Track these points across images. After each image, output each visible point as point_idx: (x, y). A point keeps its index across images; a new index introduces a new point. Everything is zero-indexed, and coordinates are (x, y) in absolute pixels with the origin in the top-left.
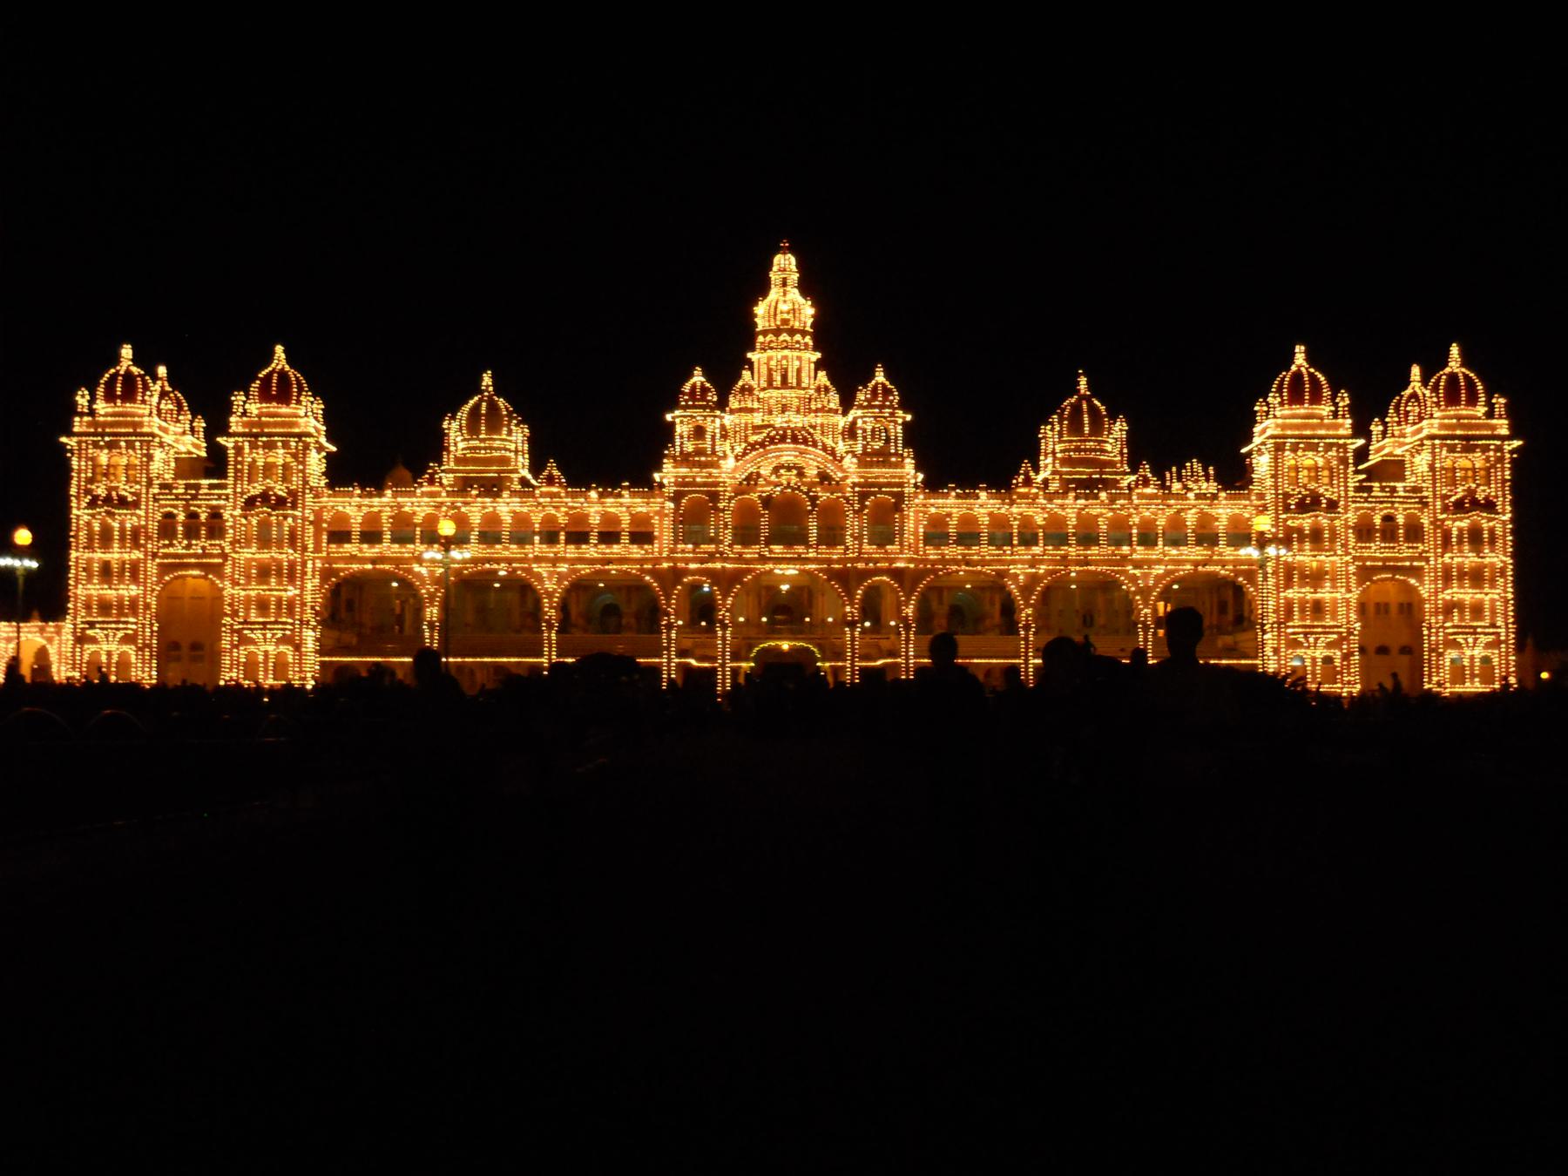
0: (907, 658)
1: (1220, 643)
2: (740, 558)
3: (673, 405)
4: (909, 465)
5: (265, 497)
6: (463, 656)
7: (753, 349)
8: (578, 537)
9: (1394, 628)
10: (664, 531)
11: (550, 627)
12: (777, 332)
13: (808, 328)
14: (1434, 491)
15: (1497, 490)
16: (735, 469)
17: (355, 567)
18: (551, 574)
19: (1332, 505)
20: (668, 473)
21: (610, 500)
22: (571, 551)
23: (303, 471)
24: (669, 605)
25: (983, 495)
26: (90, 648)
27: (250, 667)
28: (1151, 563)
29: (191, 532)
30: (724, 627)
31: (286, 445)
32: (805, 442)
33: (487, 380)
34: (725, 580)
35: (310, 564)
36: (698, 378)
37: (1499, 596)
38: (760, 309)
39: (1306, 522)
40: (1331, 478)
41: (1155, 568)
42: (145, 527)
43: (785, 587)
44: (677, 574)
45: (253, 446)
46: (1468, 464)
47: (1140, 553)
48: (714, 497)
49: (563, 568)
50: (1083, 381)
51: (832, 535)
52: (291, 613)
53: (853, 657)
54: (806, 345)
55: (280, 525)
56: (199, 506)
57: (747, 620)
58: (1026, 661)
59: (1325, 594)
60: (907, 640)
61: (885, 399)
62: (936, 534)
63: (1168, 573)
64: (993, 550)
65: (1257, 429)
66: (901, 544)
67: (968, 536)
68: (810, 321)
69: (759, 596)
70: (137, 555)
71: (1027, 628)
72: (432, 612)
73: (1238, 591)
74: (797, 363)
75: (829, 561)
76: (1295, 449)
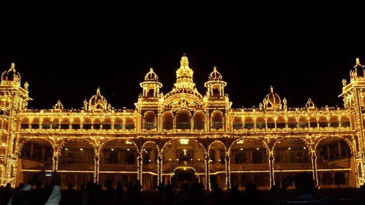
0: (228, 171)
2: (166, 135)
4: (227, 99)
7: (175, 82)
8: (107, 126)
12: (182, 77)
13: (192, 77)
16: (164, 102)
17: (31, 137)
18: (98, 140)
20: (140, 104)
21: (119, 113)
22: (104, 132)
24: (140, 152)
25: (254, 110)
28: (316, 133)
31: (7, 94)
32: (189, 92)
33: (98, 91)
36: (152, 71)
38: (178, 72)
41: (313, 136)
43: (185, 151)
47: (311, 129)
48: (156, 112)
50: (272, 89)
51: (199, 125)
54: (191, 81)
57: (173, 161)
58: (272, 171)
62: (237, 124)
63: (321, 137)
64: (258, 130)
67: (249, 125)
69: (177, 153)
71: (271, 159)
72: (56, 154)
75: (198, 135)
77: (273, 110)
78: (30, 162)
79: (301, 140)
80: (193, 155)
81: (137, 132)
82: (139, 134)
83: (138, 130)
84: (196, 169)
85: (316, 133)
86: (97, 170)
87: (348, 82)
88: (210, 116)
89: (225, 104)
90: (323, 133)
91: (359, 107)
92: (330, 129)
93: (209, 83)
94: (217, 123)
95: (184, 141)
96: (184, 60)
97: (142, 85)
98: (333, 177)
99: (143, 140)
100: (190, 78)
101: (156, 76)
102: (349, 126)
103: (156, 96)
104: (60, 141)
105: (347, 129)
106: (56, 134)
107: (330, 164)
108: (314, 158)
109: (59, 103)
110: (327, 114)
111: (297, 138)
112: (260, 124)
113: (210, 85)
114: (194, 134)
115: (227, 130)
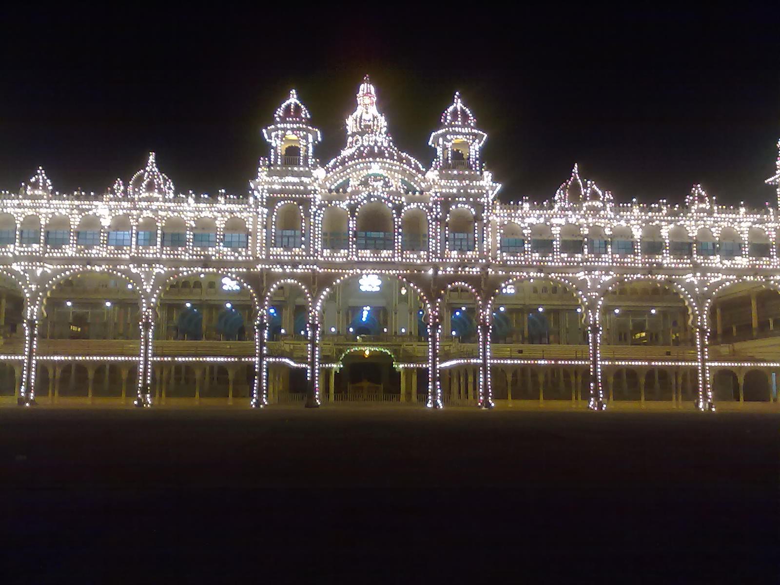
0: (485, 359)
4: (488, 175)
6: (74, 355)
12: (362, 134)
16: (326, 179)
18: (148, 275)
20: (264, 181)
24: (262, 307)
30: (314, 327)
34: (316, 282)
36: (293, 99)
48: (306, 203)
49: (159, 269)
57: (338, 333)
58: (595, 363)
67: (544, 245)
72: (32, 311)
84: (395, 352)
86: (146, 353)
93: (444, 135)
95: (370, 283)
98: (741, 380)
99: (272, 278)
101: (305, 113)
103: (306, 164)
104: (45, 277)
107: (725, 349)
108: (703, 332)
109: (41, 176)
114: (400, 263)
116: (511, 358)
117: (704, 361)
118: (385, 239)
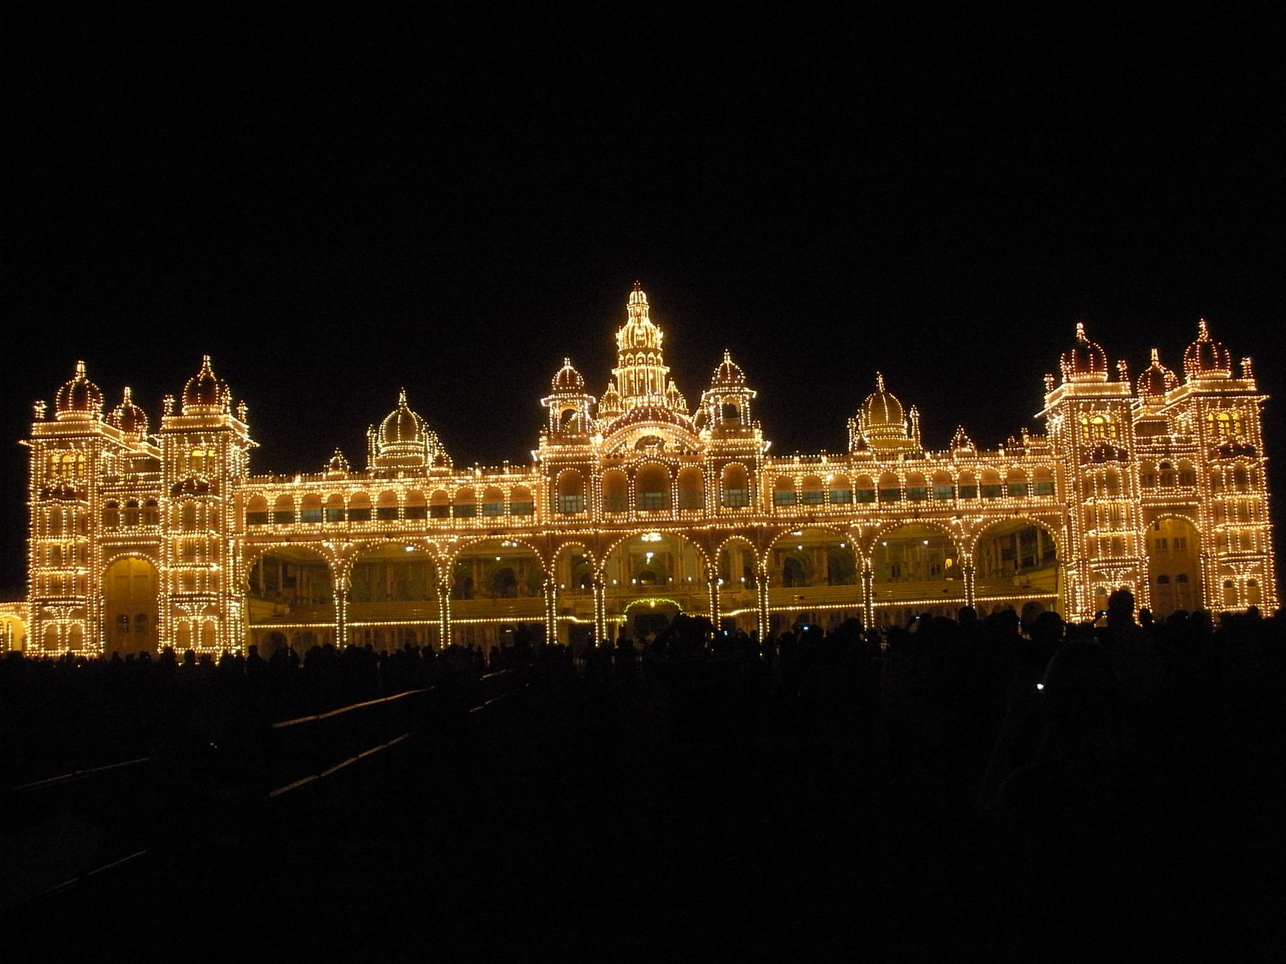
0: (763, 607)
1: (1017, 582)
2: (611, 525)
3: (547, 391)
4: (758, 434)
5: (189, 486)
8: (466, 511)
9: (1175, 563)
10: (542, 501)
11: (444, 591)
12: (635, 351)
14: (1202, 441)
15: (1251, 437)
16: (604, 444)
18: (443, 546)
19: (1123, 456)
20: (545, 451)
22: (460, 523)
23: (223, 461)
25: (824, 459)
26: (47, 623)
27: (183, 636)
28: (973, 513)
29: (131, 520)
30: (599, 587)
31: (208, 440)
32: (665, 418)
33: (402, 397)
35: (232, 543)
36: (568, 367)
37: (1261, 527)
38: (620, 335)
39: (1101, 469)
40: (1118, 432)
41: (969, 518)
42: (91, 515)
43: (650, 555)
44: (554, 542)
45: (180, 441)
46: (1227, 418)
47: (961, 503)
48: (586, 470)
50: (880, 380)
51: (692, 500)
52: (216, 587)
53: (715, 608)
55: (203, 509)
56: (136, 496)
57: (619, 583)
58: (868, 605)
59: (1123, 533)
60: (763, 591)
61: (733, 380)
63: (985, 521)
64: (836, 507)
65: (1047, 397)
66: (755, 506)
68: (660, 343)
69: (629, 562)
70: (83, 539)
71: (867, 575)
72: (340, 583)
73: (1044, 532)
74: (651, 376)
75: (690, 524)
76: (1086, 409)
77: (870, 458)
78: (264, 604)
79: (940, 529)
80: (671, 568)
81: (539, 521)
82: (547, 527)
83: (544, 516)
85: (973, 513)
86: (445, 617)
87: (1057, 384)
88: (718, 476)
89: (751, 445)
90: (991, 511)
91: (1075, 448)
92: (1006, 502)
93: (714, 395)
94: (735, 491)
96: (638, 301)
97: (547, 402)
98: (1019, 613)
100: (656, 351)
101: (579, 380)
102: (1054, 494)
103: (584, 430)
105: (1047, 501)
106: (340, 535)
108: (969, 570)
109: (338, 457)
110: (1001, 464)
111: (929, 524)
112: (840, 493)
113: (712, 401)
114: (679, 522)
115: (761, 508)
116: (793, 605)
117: (970, 598)
118: (662, 498)
